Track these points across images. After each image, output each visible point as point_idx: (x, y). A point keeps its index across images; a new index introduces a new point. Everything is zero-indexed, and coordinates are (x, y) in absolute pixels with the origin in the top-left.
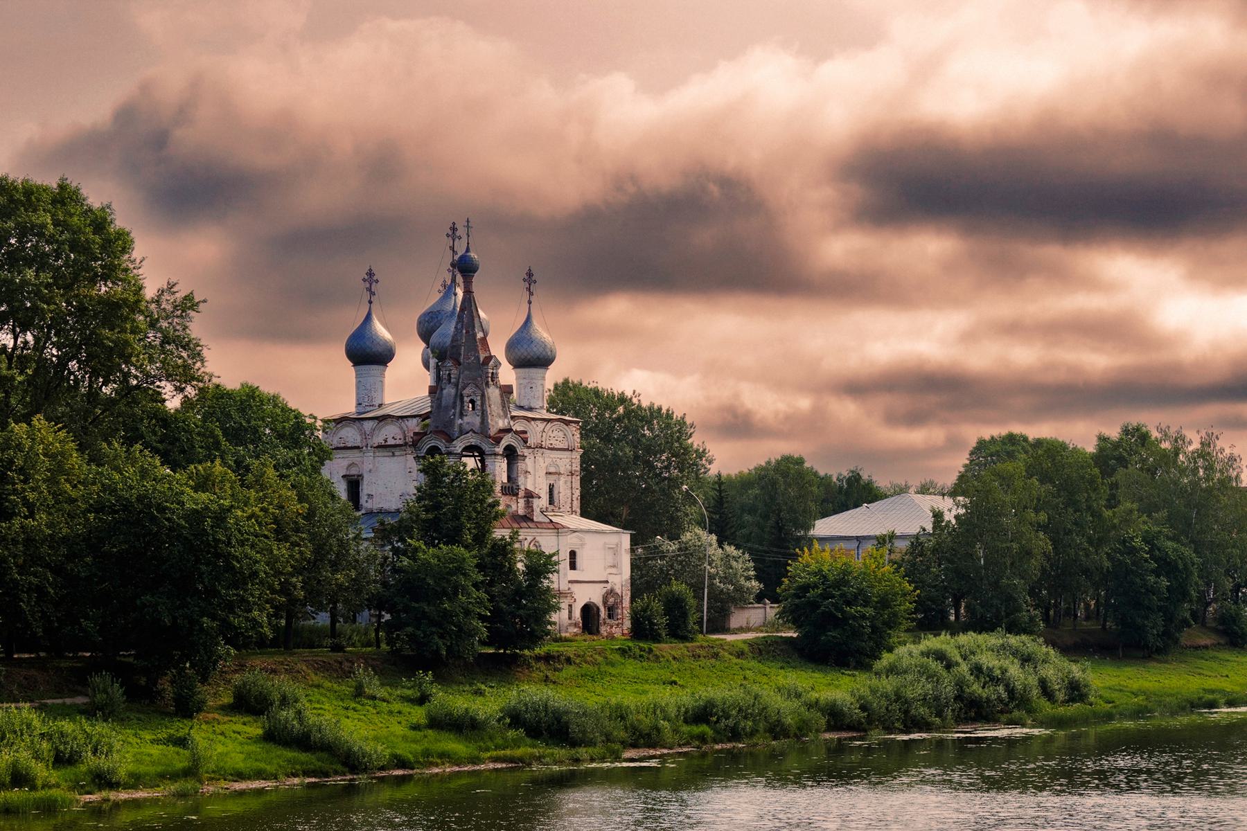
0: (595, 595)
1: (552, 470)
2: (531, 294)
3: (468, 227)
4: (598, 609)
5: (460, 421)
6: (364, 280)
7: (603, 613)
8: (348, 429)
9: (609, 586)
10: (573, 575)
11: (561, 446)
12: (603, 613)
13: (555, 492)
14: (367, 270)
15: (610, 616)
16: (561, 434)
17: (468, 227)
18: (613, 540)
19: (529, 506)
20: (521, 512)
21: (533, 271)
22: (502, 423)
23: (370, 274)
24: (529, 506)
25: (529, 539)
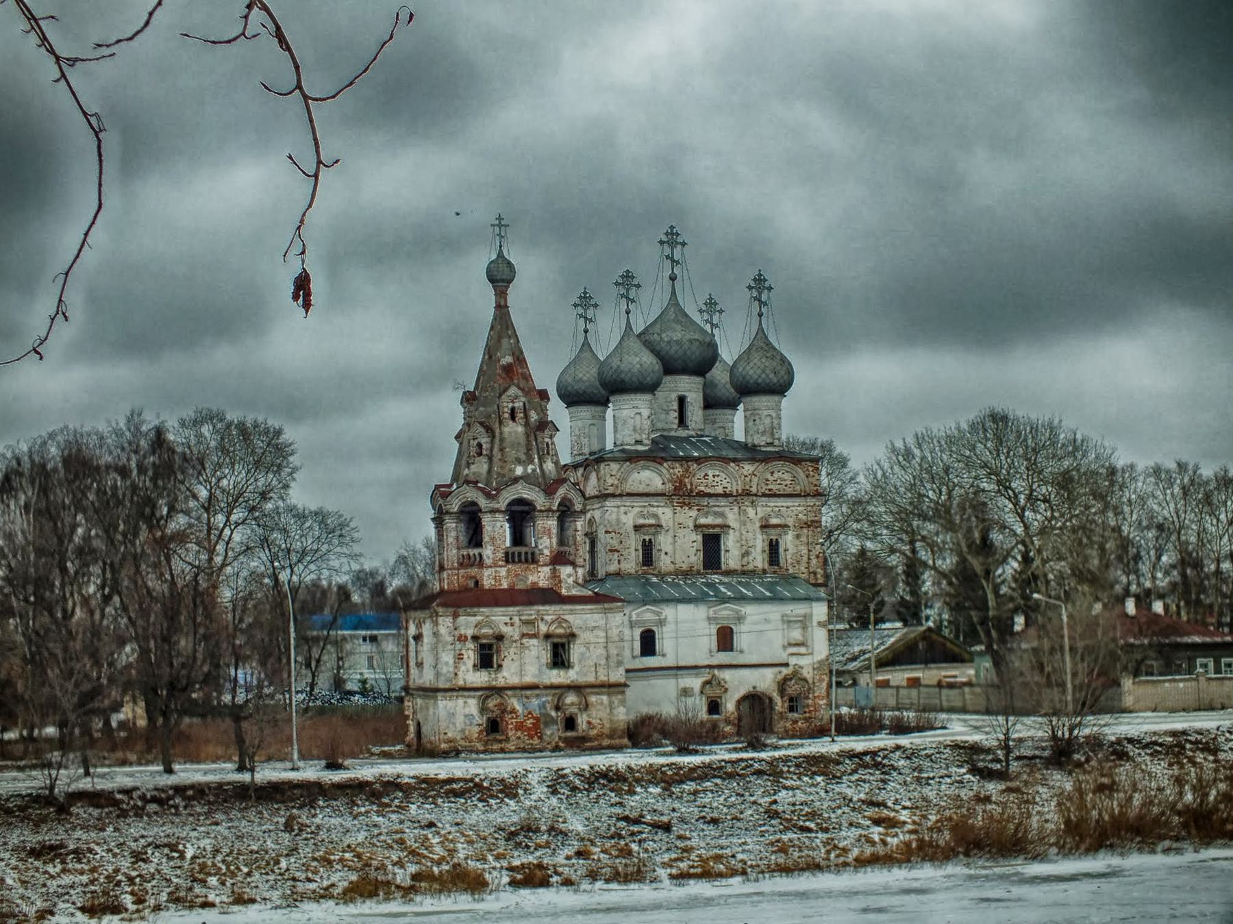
0: (765, 681)
1: (774, 521)
4: (771, 699)
5: (466, 471)
7: (780, 704)
9: (785, 671)
10: (724, 658)
11: (789, 491)
12: (780, 704)
15: (791, 709)
16: (787, 476)
17: (500, 226)
18: (799, 609)
19: (555, 576)
20: (543, 583)
22: (519, 471)
24: (555, 576)
25: (549, 618)
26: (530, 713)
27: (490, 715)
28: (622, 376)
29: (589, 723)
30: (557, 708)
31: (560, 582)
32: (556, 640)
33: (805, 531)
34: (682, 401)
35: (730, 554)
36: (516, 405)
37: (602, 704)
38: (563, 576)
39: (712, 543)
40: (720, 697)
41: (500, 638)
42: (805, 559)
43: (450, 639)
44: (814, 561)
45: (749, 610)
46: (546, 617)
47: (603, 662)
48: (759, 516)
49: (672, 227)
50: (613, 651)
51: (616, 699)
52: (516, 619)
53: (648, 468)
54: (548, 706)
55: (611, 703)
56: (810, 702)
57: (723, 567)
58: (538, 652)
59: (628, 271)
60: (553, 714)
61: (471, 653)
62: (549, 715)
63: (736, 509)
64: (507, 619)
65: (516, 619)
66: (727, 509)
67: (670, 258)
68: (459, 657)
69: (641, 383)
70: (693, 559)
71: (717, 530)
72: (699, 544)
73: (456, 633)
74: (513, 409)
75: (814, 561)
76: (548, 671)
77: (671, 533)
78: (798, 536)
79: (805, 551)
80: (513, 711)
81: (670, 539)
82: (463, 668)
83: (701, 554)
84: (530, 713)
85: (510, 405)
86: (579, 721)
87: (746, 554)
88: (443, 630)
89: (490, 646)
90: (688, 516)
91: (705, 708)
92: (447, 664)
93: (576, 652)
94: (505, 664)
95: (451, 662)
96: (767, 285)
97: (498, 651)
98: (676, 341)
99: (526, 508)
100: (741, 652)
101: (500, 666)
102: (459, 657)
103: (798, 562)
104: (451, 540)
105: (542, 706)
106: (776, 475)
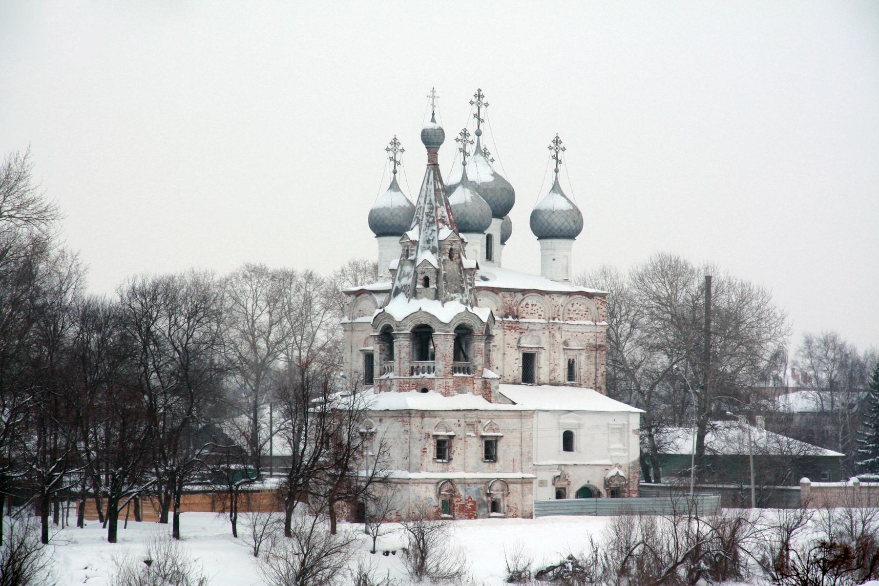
2: (558, 162)
3: (433, 97)
6: (388, 150)
8: (366, 302)
13: (576, 368)
14: (391, 139)
17: (433, 97)
21: (561, 138)
23: (395, 142)
26: (470, 498)
27: (444, 498)
28: (467, 218)
29: (508, 506)
30: (488, 495)
31: (490, 392)
32: (440, 438)
33: (594, 353)
34: (489, 238)
35: (541, 370)
36: (454, 247)
37: (516, 491)
38: (492, 388)
39: (528, 360)
40: (565, 489)
41: (452, 437)
42: (593, 376)
43: (418, 436)
44: (600, 379)
45: (586, 420)
46: (482, 421)
47: (518, 458)
48: (563, 340)
49: (479, 90)
50: (525, 450)
51: (527, 487)
52: (462, 421)
53: (487, 296)
54: (482, 492)
55: (522, 490)
56: (626, 495)
57: (536, 381)
58: (476, 449)
59: (465, 130)
60: (485, 498)
61: (432, 448)
62: (482, 500)
63: (547, 333)
64: (456, 421)
65: (462, 421)
66: (540, 333)
67: (480, 120)
68: (424, 451)
69: (480, 225)
70: (516, 373)
71: (533, 351)
72: (520, 363)
73: (423, 431)
74: (451, 249)
75: (600, 379)
76: (482, 463)
77: (501, 351)
78: (588, 357)
79: (594, 370)
80: (459, 496)
81: (500, 356)
82: (426, 460)
83: (521, 369)
84: (470, 498)
85: (450, 247)
86: (502, 505)
87: (552, 371)
88: (414, 429)
89: (444, 442)
90: (512, 337)
91: (554, 495)
92: (416, 456)
93: (501, 449)
94: (454, 456)
95: (419, 454)
96: (562, 146)
97: (450, 447)
98: (491, 190)
99: (464, 332)
100: (580, 452)
101: (450, 459)
102: (424, 451)
103: (588, 379)
104: (403, 355)
105: (478, 492)
106: (576, 306)
